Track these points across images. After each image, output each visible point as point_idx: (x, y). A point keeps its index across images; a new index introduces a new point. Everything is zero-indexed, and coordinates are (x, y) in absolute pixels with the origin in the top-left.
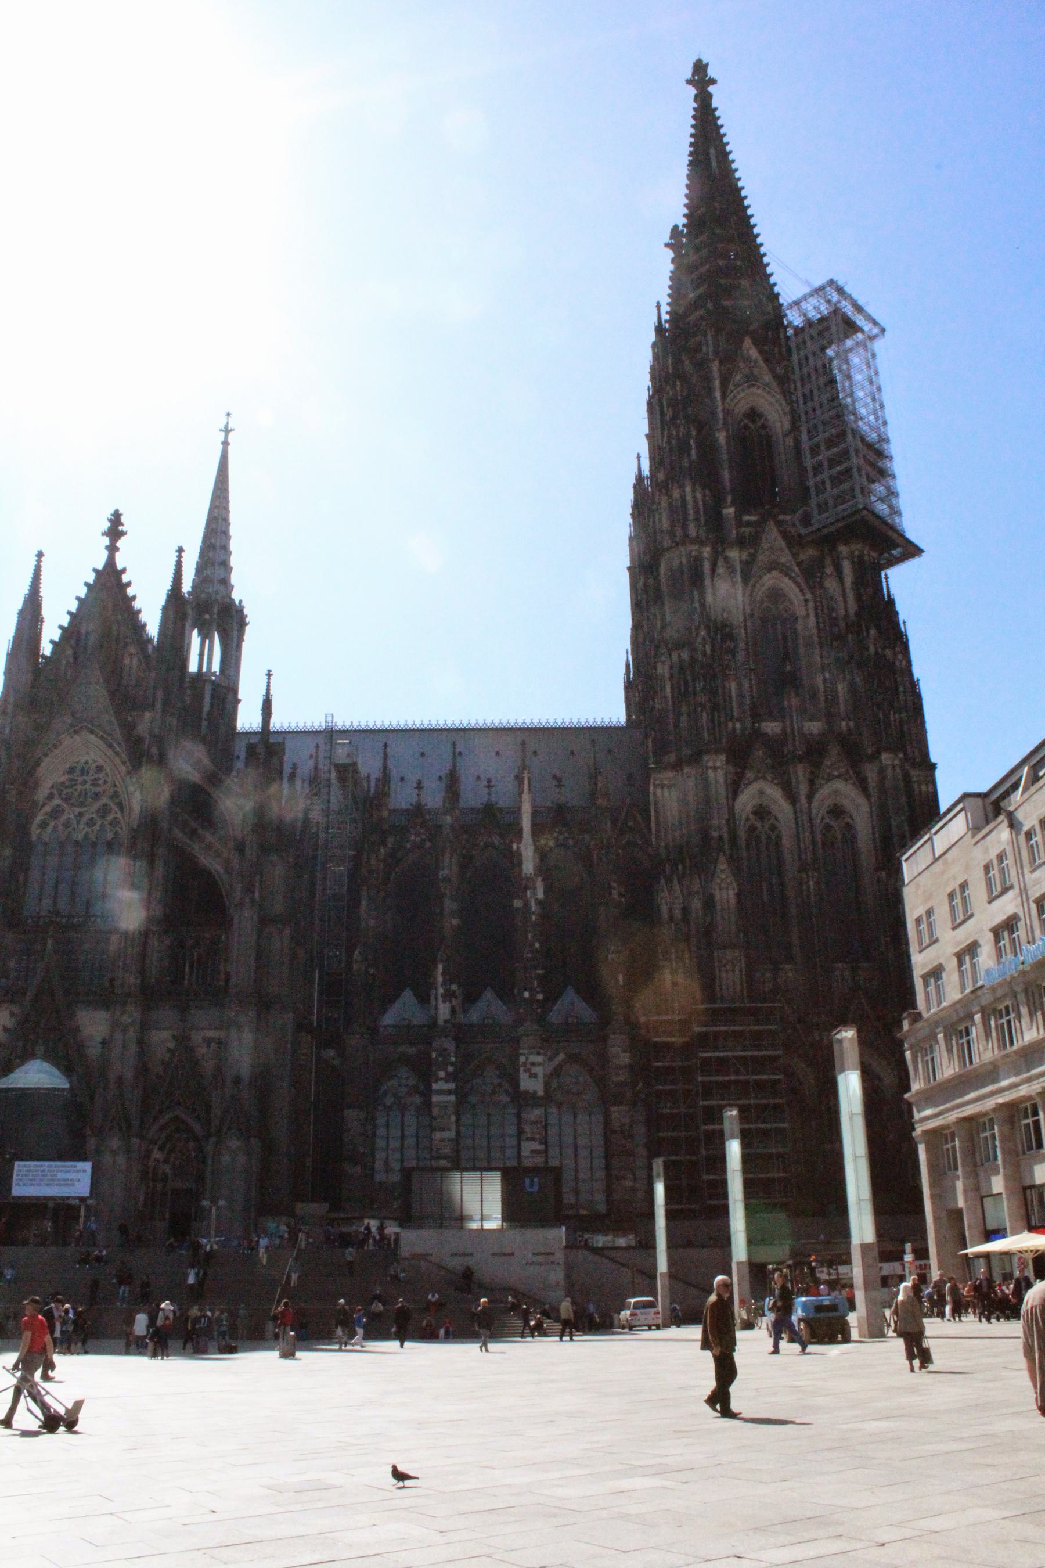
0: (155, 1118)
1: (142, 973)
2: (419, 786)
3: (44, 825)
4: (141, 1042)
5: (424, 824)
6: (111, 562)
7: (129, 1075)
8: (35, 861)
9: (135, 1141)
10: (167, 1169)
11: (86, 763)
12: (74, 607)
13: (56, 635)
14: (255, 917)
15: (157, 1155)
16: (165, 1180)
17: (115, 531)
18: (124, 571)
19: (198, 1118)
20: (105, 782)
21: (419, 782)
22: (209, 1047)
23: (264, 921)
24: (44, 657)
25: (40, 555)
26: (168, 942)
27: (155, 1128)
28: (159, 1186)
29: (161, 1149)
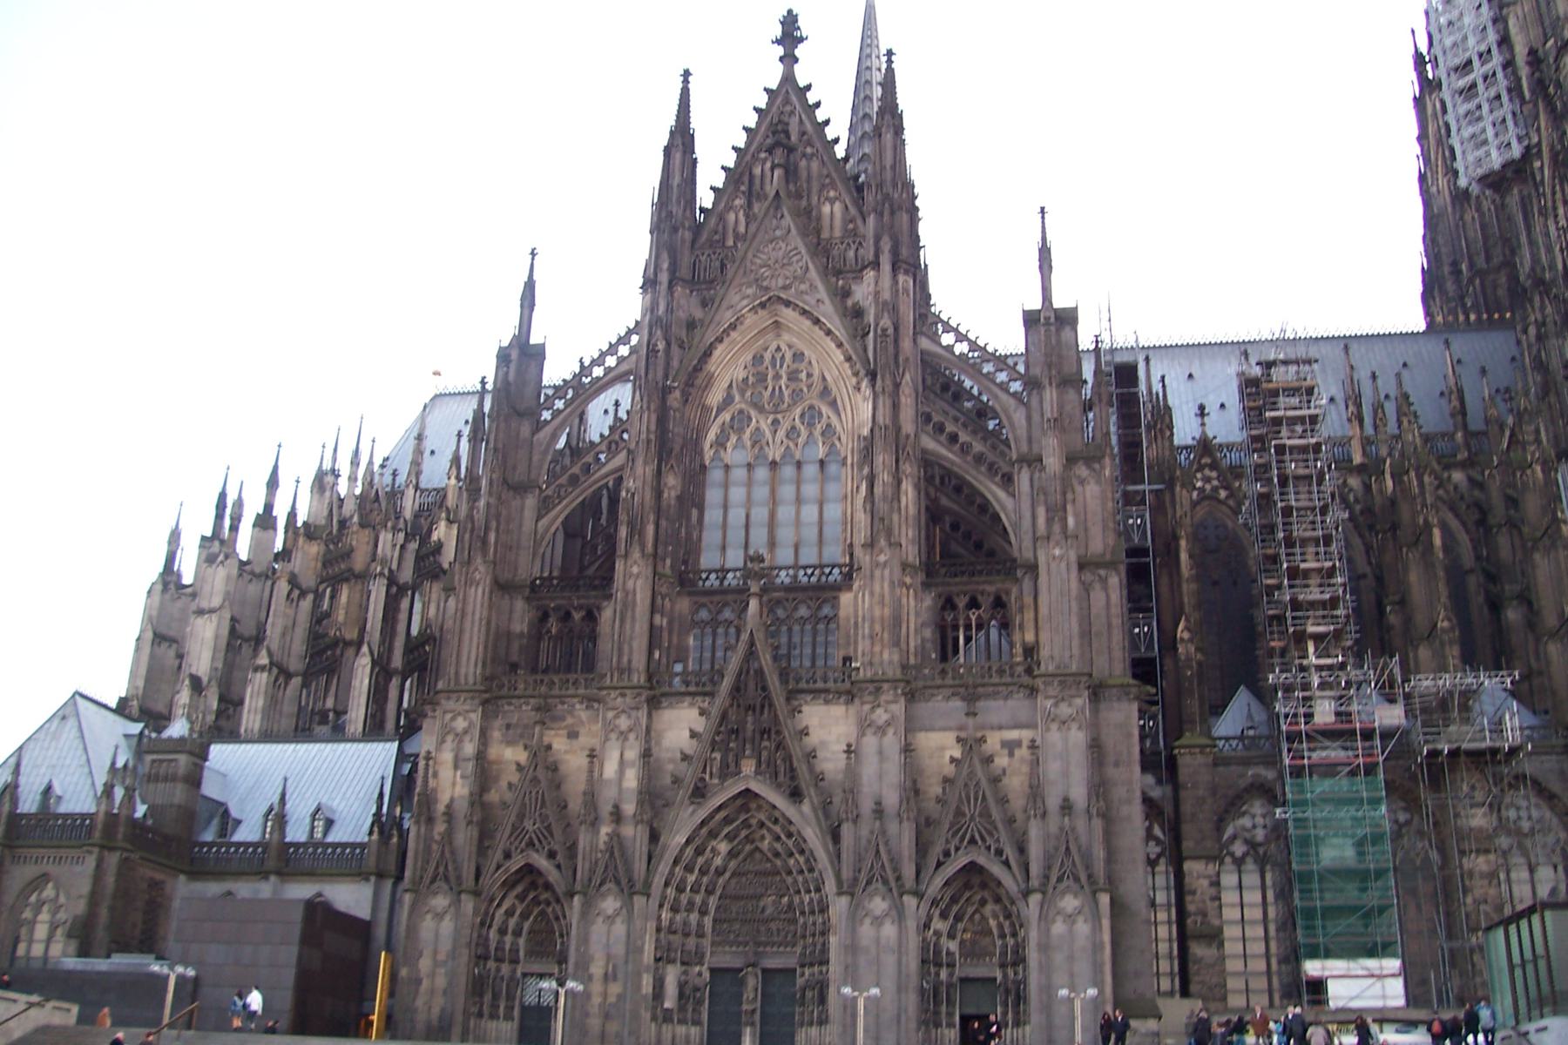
0: (939, 864)
1: (897, 644)
2: (1202, 411)
3: (720, 443)
4: (908, 749)
5: (1214, 466)
6: (788, 78)
7: (891, 799)
8: (713, 496)
9: (910, 901)
10: (953, 946)
11: (778, 349)
12: (741, 140)
13: (719, 180)
14: (1073, 556)
15: (938, 924)
16: (951, 965)
17: (790, 35)
18: (809, 87)
19: (1007, 863)
20: (809, 375)
21: (1202, 408)
22: (1011, 754)
23: (1082, 566)
24: (702, 210)
25: (687, 74)
26: (928, 601)
27: (939, 881)
28: (944, 974)
29: (944, 916)
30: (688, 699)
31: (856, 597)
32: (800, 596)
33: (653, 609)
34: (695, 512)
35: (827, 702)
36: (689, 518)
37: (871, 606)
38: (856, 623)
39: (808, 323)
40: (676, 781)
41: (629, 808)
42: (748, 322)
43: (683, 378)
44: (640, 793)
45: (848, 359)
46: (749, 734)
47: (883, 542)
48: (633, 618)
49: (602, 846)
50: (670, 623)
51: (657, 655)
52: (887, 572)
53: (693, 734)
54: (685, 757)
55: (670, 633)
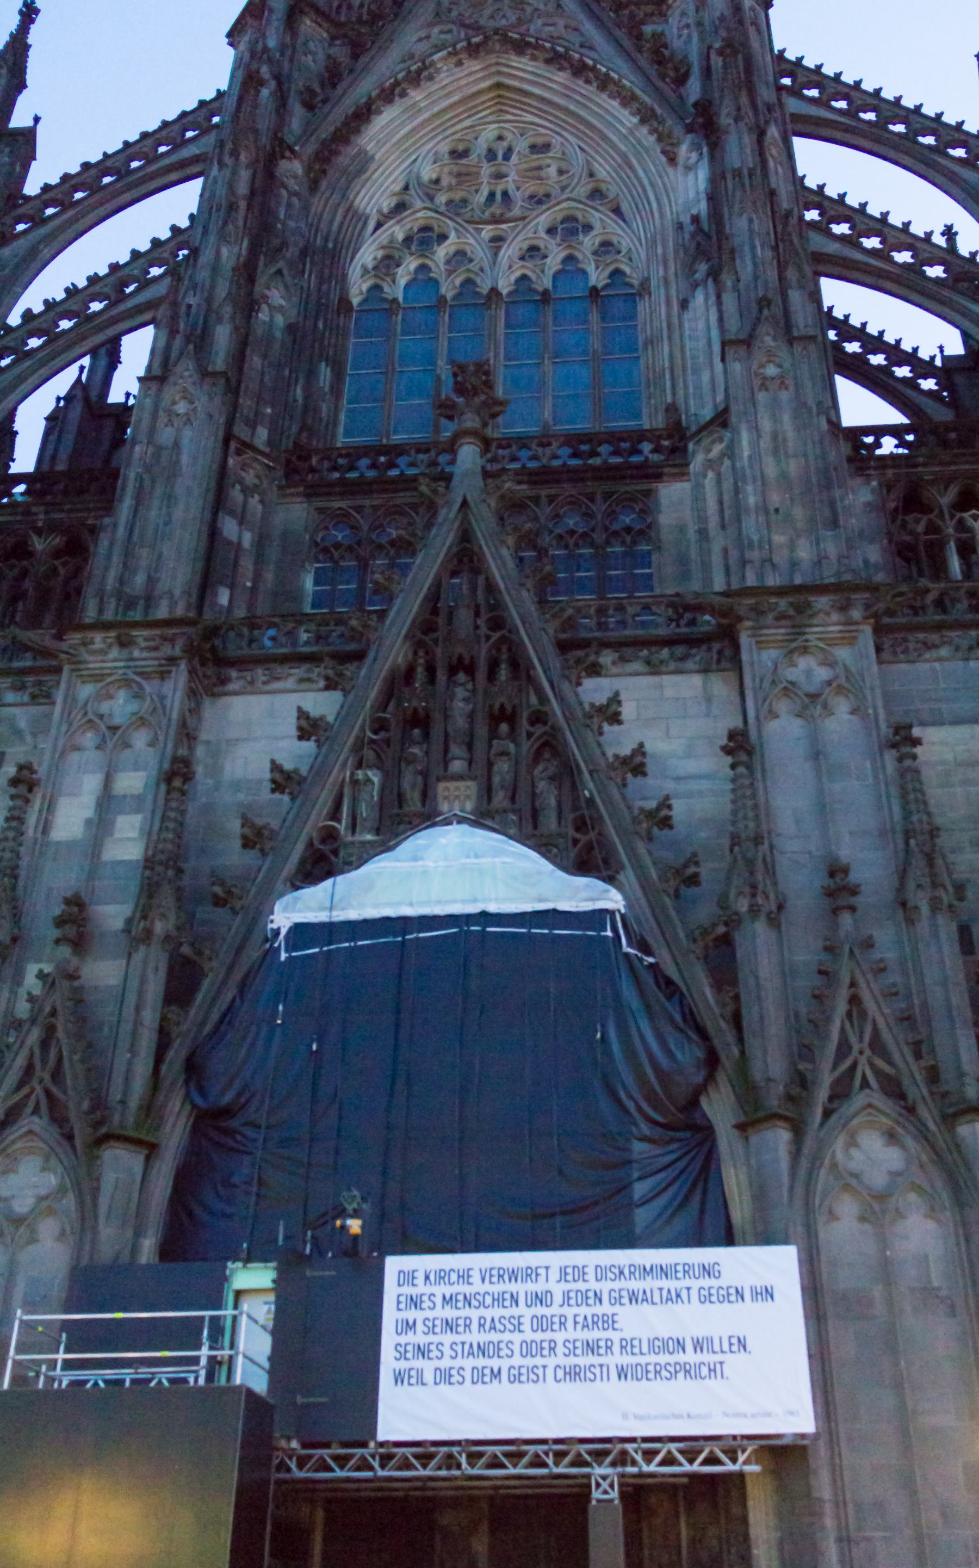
7: (871, 868)
30: (299, 671)
31: (698, 487)
32: (568, 489)
33: (218, 502)
34: (325, 373)
35: (654, 669)
36: (312, 374)
37: (756, 457)
38: (703, 533)
39: (562, 77)
40: (255, 838)
41: (113, 914)
42: (443, 78)
43: (311, 148)
44: (149, 863)
45: (647, 116)
46: (460, 722)
47: (769, 341)
48: (170, 498)
49: (23, 1009)
50: (261, 542)
51: (224, 597)
52: (785, 396)
53: (309, 727)
54: (283, 780)
55: (260, 559)
